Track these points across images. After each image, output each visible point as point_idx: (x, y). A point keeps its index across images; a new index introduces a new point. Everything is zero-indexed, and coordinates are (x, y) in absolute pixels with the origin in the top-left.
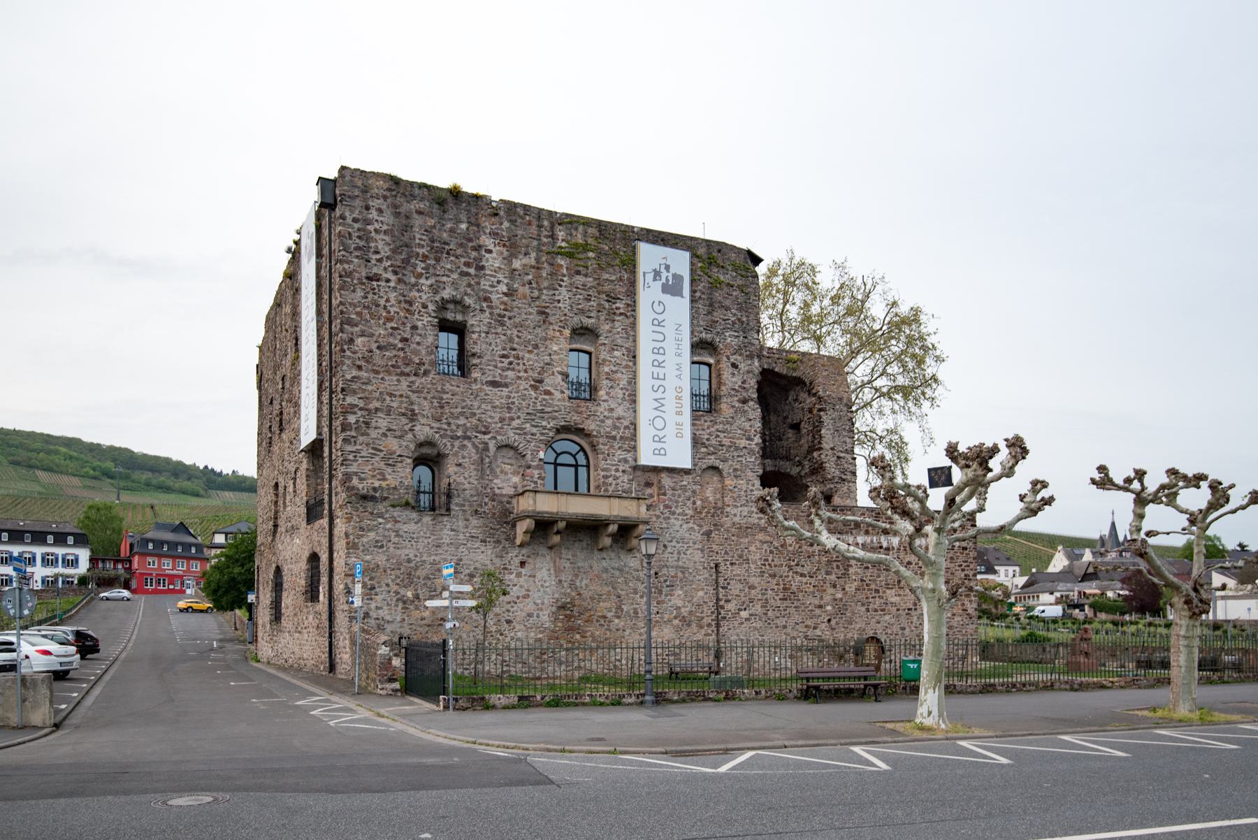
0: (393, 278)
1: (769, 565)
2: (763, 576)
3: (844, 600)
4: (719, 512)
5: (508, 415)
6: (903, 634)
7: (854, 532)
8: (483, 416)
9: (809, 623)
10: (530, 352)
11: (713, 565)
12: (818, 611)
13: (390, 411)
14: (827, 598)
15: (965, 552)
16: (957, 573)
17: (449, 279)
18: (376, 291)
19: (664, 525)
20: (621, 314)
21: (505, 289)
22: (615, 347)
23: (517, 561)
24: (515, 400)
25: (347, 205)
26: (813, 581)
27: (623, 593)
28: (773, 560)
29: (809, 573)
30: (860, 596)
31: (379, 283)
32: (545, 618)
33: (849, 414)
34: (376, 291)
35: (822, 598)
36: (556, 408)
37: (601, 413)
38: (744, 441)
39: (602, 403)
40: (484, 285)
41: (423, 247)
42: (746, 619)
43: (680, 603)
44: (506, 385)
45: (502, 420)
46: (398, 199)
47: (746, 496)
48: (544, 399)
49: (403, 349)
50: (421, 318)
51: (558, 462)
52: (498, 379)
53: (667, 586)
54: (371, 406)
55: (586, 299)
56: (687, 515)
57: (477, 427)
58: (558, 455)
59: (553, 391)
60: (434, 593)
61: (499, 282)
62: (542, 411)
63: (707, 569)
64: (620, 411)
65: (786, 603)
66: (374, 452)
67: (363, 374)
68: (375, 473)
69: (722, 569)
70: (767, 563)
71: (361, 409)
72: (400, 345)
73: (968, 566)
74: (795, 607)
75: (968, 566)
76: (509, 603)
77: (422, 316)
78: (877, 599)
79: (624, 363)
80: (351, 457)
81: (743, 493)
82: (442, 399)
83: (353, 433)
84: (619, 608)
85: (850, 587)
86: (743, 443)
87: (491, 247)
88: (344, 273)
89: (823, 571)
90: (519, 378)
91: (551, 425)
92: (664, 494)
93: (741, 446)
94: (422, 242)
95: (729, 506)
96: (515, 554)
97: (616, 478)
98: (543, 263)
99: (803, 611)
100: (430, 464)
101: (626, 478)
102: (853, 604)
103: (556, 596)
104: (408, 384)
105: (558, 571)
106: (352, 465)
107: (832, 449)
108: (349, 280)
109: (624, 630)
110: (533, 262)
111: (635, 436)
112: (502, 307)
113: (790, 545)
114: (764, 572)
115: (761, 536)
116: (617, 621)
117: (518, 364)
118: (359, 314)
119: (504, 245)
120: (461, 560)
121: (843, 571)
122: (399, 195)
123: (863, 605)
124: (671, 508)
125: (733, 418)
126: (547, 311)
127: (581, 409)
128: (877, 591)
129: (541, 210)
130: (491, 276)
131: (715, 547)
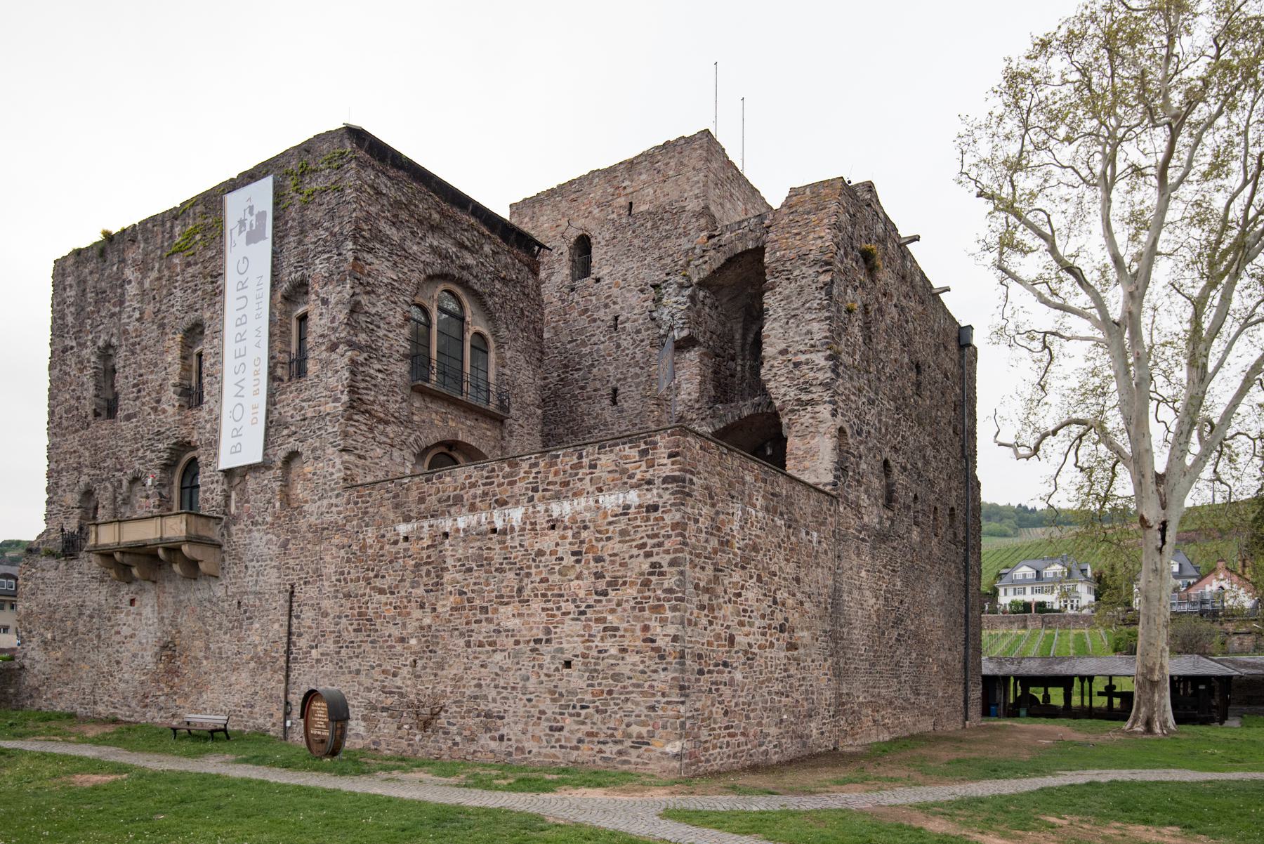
1: (345, 579)
2: (336, 597)
3: (433, 628)
6: (524, 687)
7: (453, 510)
9: (388, 666)
12: (399, 648)
14: (412, 626)
15: (653, 515)
16: (634, 563)
19: (248, 541)
23: (127, 598)
26: (392, 599)
27: (211, 629)
28: (349, 573)
30: (459, 622)
32: (149, 658)
42: (318, 661)
43: (256, 639)
65: (362, 636)
70: (342, 577)
73: (660, 545)
74: (371, 642)
75: (660, 545)
76: (119, 643)
78: (484, 624)
84: (207, 648)
85: (444, 606)
89: (407, 584)
92: (247, 502)
95: (306, 502)
99: (381, 647)
101: (219, 488)
102: (446, 635)
103: (159, 634)
105: (161, 606)
113: (371, 547)
116: (205, 662)
121: (435, 580)
123: (462, 635)
125: (318, 376)
128: (484, 610)
131: (291, 562)
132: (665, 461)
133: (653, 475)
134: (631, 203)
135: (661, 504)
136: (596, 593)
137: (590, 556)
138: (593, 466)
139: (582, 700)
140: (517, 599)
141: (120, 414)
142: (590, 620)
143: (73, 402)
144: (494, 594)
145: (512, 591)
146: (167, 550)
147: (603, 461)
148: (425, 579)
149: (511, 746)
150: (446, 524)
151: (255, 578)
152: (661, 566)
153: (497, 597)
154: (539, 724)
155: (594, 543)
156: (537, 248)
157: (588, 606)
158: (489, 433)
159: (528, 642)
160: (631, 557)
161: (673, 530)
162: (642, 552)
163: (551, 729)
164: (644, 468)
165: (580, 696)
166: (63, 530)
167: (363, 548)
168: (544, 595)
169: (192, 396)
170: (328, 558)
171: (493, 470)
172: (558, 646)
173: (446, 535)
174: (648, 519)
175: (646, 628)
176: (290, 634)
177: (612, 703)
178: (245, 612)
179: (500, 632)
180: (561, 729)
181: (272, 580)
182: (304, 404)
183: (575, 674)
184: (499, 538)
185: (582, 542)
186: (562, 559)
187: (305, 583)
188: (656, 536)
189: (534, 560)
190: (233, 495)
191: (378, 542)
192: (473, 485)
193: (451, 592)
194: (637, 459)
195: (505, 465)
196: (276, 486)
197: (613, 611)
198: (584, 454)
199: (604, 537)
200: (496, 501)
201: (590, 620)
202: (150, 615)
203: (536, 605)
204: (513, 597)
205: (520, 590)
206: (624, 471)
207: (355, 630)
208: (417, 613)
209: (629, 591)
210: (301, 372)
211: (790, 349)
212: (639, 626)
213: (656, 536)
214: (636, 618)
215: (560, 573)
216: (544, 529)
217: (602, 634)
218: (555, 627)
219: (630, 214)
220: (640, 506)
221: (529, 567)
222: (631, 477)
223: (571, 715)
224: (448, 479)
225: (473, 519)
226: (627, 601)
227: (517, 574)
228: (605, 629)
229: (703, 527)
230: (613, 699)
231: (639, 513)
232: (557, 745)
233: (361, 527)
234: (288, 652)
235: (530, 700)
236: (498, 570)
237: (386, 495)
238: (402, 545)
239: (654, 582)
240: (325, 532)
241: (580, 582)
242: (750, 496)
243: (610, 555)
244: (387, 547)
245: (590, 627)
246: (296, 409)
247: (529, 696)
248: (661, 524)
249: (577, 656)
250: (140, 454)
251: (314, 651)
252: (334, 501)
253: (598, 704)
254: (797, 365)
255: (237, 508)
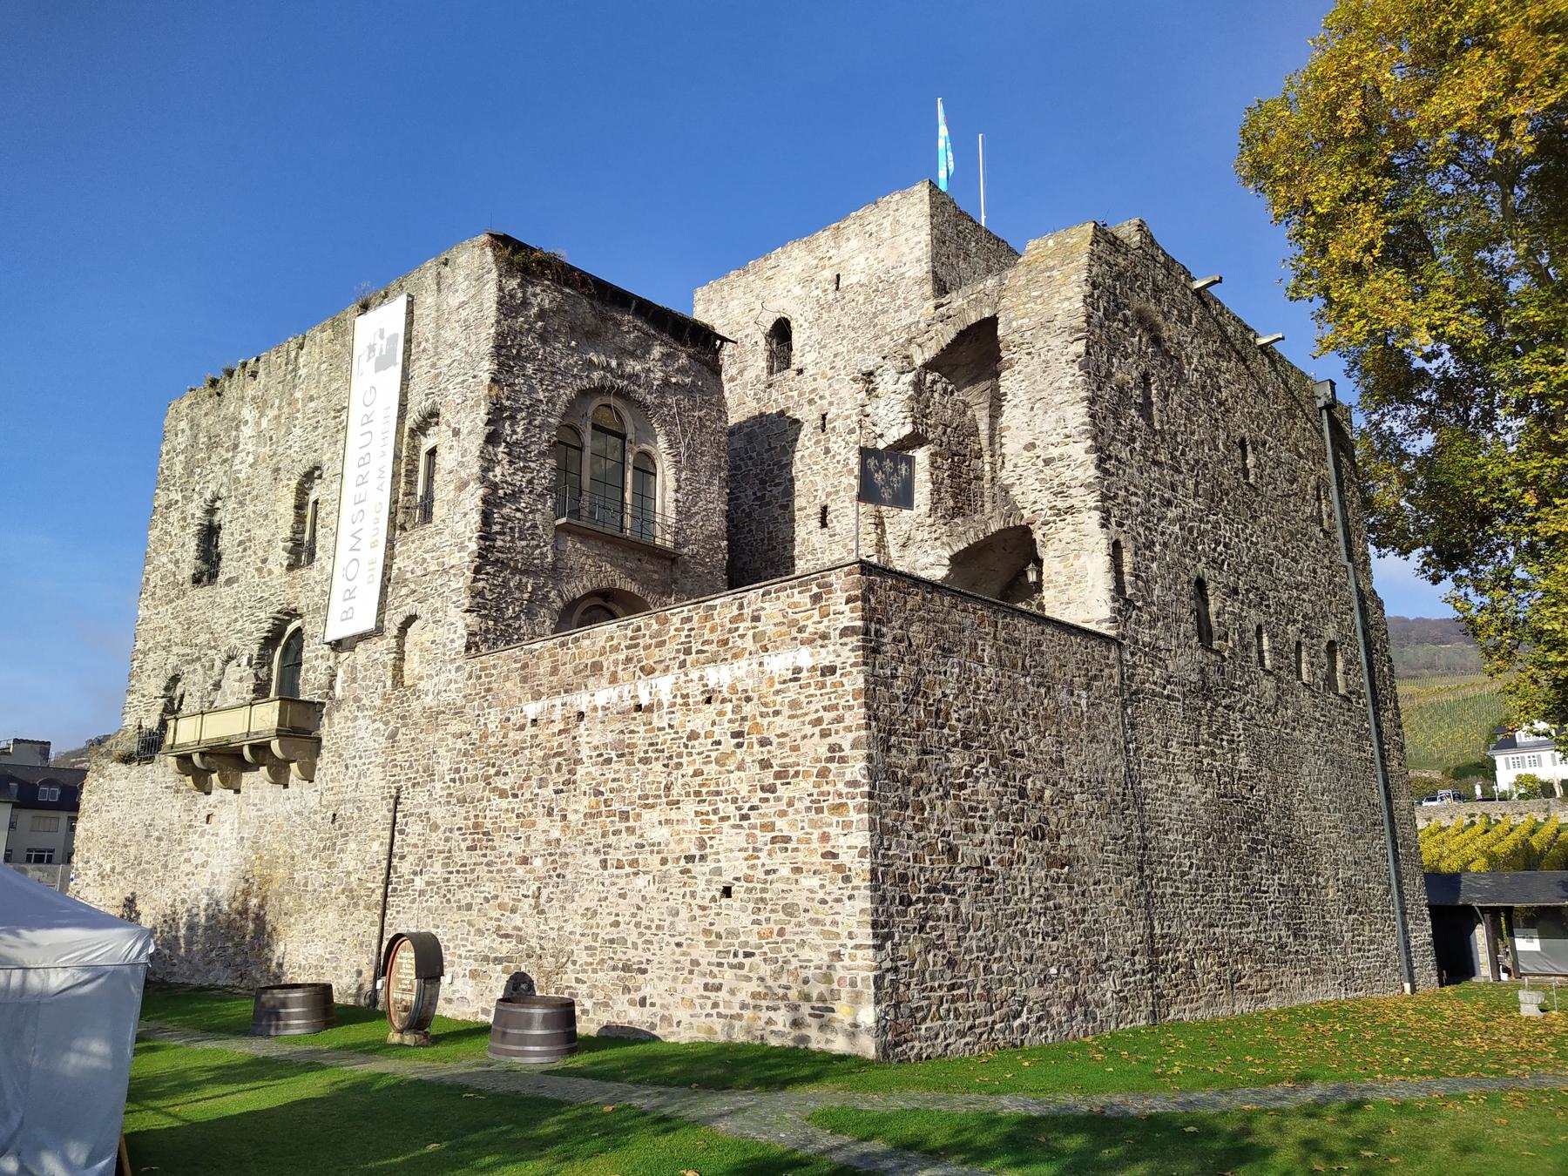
2: (449, 802)
3: (562, 843)
12: (520, 871)
15: (829, 680)
16: (806, 746)
27: (297, 852)
28: (466, 770)
30: (593, 831)
70: (457, 776)
73: (840, 720)
74: (488, 864)
75: (840, 720)
89: (534, 783)
99: (499, 871)
107: (1031, 446)
115: (455, 726)
121: (567, 777)
123: (597, 851)
128: (625, 816)
131: (399, 757)
133: (828, 627)
134: (838, 276)
135: (839, 665)
136: (763, 789)
137: (755, 738)
138: (756, 619)
139: (746, 944)
140: (664, 800)
141: (222, 578)
142: (754, 827)
143: (171, 566)
144: (636, 794)
145: (658, 789)
146: (253, 747)
147: (768, 611)
148: (555, 775)
149: (655, 1014)
150: (582, 701)
151: (355, 781)
152: (841, 750)
153: (640, 797)
154: (690, 981)
155: (759, 719)
156: (718, 342)
157: (752, 808)
158: (656, 576)
159: (678, 859)
160: (804, 737)
161: (855, 699)
162: (817, 730)
163: (706, 987)
164: (816, 618)
165: (743, 938)
166: (140, 727)
167: (484, 737)
168: (698, 794)
169: (301, 552)
170: (442, 752)
171: (639, 629)
172: (715, 865)
173: (581, 715)
174: (823, 686)
175: (825, 838)
176: (391, 854)
177: (784, 947)
178: (341, 828)
179: (643, 846)
180: (718, 988)
181: (375, 783)
182: (426, 556)
183: (737, 905)
185: (744, 719)
186: (718, 743)
187: (414, 785)
188: (835, 707)
189: (686, 746)
190: (340, 673)
191: (502, 727)
192: (615, 649)
193: (585, 793)
194: (809, 606)
195: (653, 621)
196: (389, 659)
197: (783, 814)
198: (746, 602)
199: (770, 710)
201: (754, 827)
202: (228, 836)
203: (689, 807)
204: (659, 797)
205: (668, 788)
206: (793, 623)
208: (543, 823)
209: (803, 784)
210: (427, 516)
211: (1037, 443)
212: (816, 834)
213: (835, 707)
214: (814, 824)
215: (717, 762)
216: (696, 703)
217: (770, 846)
218: (711, 838)
219: (837, 288)
220: (814, 669)
221: (680, 755)
222: (800, 630)
223: (731, 966)
224: (586, 642)
226: (800, 799)
227: (666, 766)
228: (774, 840)
229: (899, 692)
230: (785, 942)
231: (812, 677)
232: (714, 1012)
234: (387, 882)
235: (679, 945)
236: (645, 761)
237: (515, 666)
238: (530, 730)
239: (834, 771)
240: (440, 717)
241: (742, 774)
242: (974, 647)
243: (778, 736)
244: (511, 734)
245: (754, 836)
246: (416, 563)
247: (678, 939)
248: (840, 690)
249: (737, 879)
250: (238, 626)
251: (417, 879)
252: (453, 675)
253: (766, 949)
254: (1047, 462)
255: (343, 688)
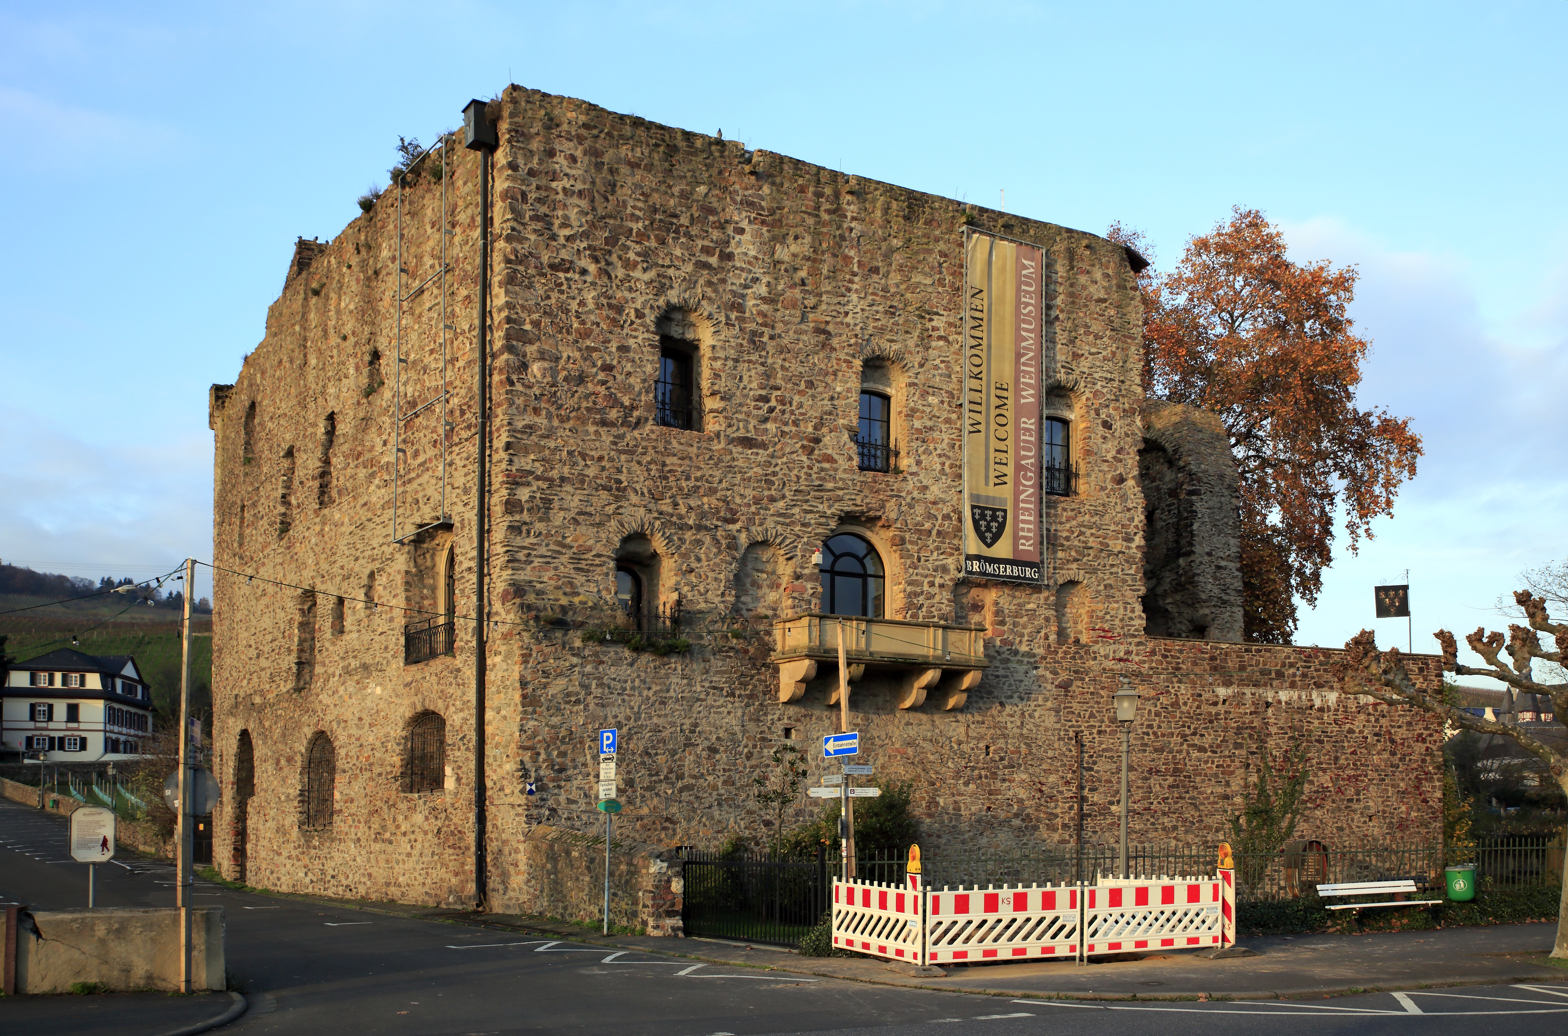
0: (592, 268)
1: (1155, 733)
2: (1145, 751)
4: (1082, 652)
5: (766, 493)
7: (1275, 683)
8: (729, 493)
10: (801, 393)
11: (1072, 734)
13: (582, 482)
17: (677, 273)
18: (564, 287)
19: (1001, 672)
20: (940, 338)
21: (763, 290)
22: (931, 390)
24: (777, 469)
25: (520, 148)
28: (1159, 727)
29: (1211, 746)
31: (569, 275)
33: (1234, 500)
34: (564, 287)
35: (1228, 784)
36: (840, 484)
37: (909, 493)
38: (1120, 541)
39: (909, 478)
40: (732, 284)
41: (638, 219)
44: (764, 446)
45: (757, 501)
46: (600, 141)
47: (1122, 628)
48: (822, 469)
49: (603, 383)
50: (634, 333)
51: (837, 568)
52: (751, 434)
53: (1005, 767)
54: (555, 474)
55: (886, 312)
56: (1034, 656)
57: (718, 510)
58: (837, 558)
59: (836, 457)
60: (654, 778)
61: (756, 280)
62: (820, 488)
63: (1063, 739)
64: (935, 491)
66: (557, 548)
67: (541, 421)
68: (560, 583)
69: (1086, 739)
70: (1151, 732)
71: (538, 478)
72: (601, 376)
77: (635, 330)
79: (945, 415)
80: (521, 556)
81: (1117, 622)
82: (664, 464)
83: (526, 516)
86: (1117, 545)
87: (744, 224)
88: (513, 257)
90: (783, 434)
91: (833, 510)
93: (1116, 550)
94: (637, 213)
96: (776, 717)
97: (931, 597)
98: (823, 253)
100: (636, 568)
104: (611, 439)
106: (523, 569)
108: (521, 268)
109: (939, 837)
110: (807, 250)
111: (960, 530)
112: (760, 320)
114: (1146, 745)
117: (783, 412)
118: (536, 324)
119: (763, 223)
120: (696, 725)
122: (602, 135)
124: (1012, 644)
126: (830, 328)
127: (878, 486)
129: (820, 169)
130: (742, 270)
132: (1433, 678)
173: (1268, 705)
184: (1318, 714)
191: (1194, 700)
200: (1315, 683)
207: (1170, 787)
225: (1294, 694)
233: (1172, 682)
